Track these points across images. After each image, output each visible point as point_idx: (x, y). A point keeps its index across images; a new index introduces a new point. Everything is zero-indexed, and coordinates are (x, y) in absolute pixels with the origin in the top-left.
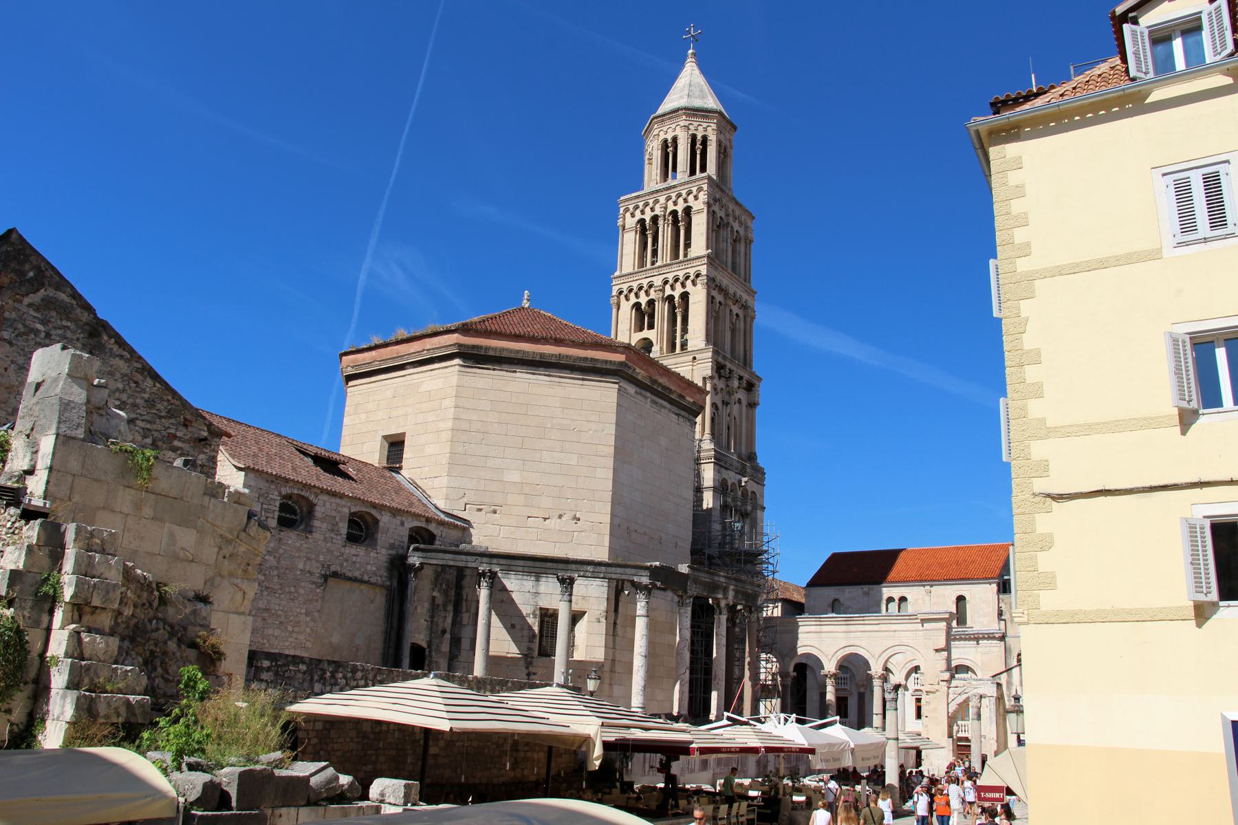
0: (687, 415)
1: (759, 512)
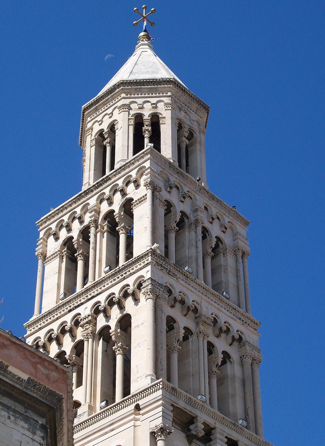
0: (20, 408)
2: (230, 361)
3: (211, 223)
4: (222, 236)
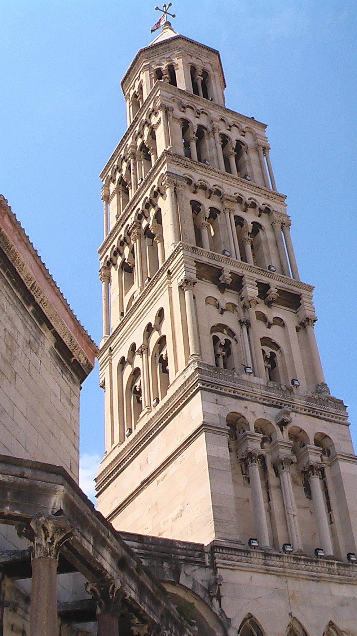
1: (344, 467)
2: (262, 229)
3: (230, 130)
4: (242, 139)
